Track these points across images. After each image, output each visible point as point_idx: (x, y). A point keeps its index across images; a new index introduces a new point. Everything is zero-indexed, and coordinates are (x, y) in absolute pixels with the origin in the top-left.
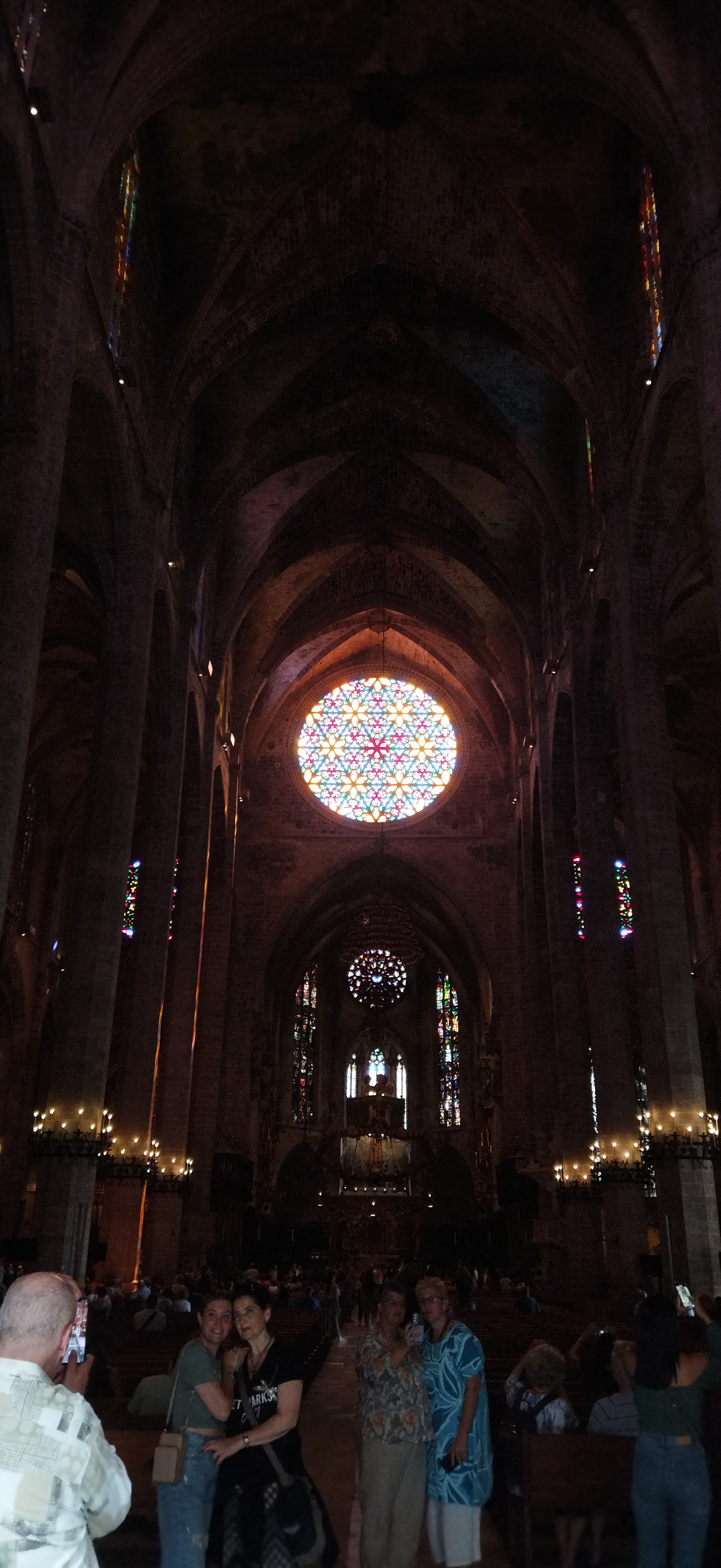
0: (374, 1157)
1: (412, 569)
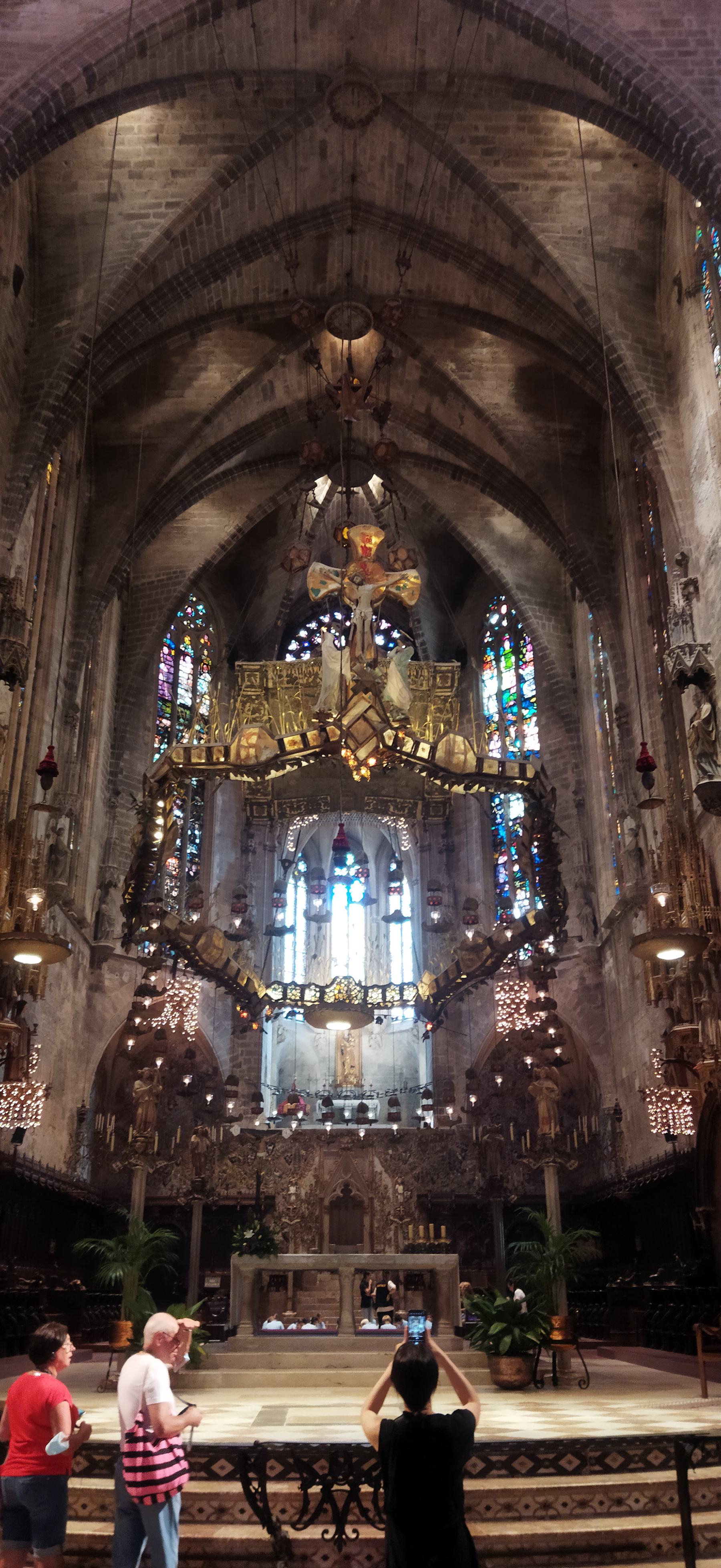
0: (344, 1064)
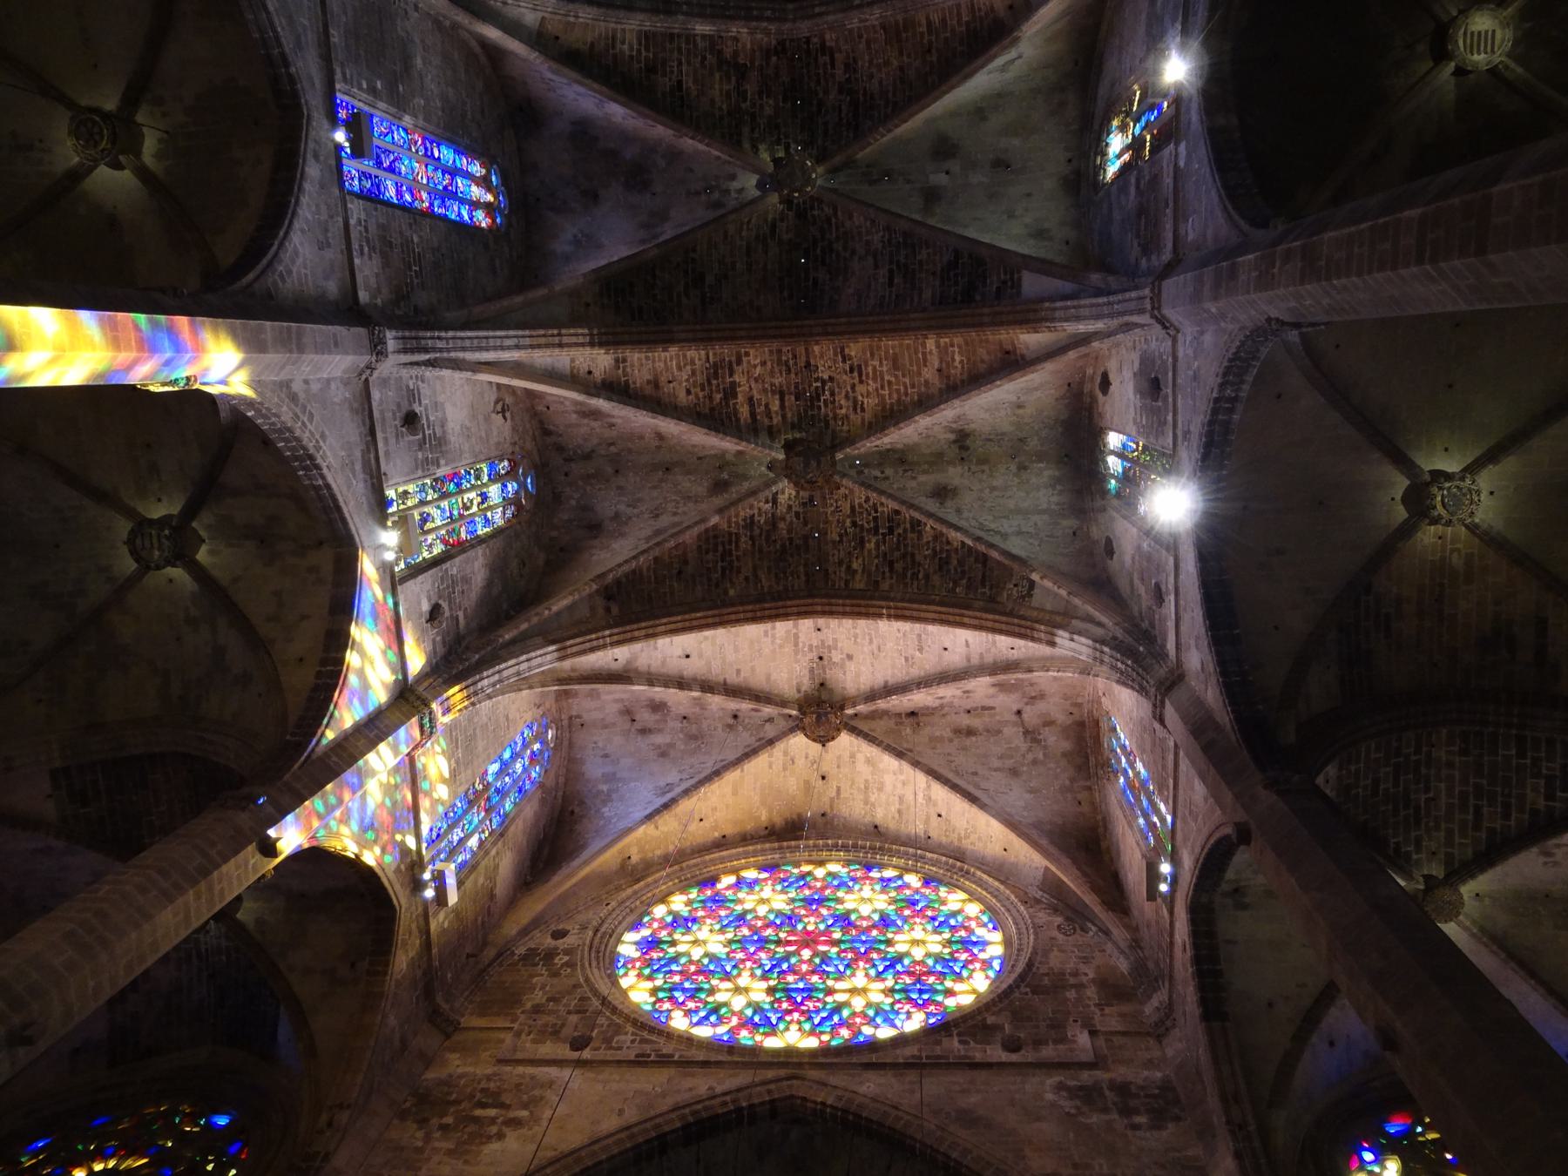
1: (876, 532)
